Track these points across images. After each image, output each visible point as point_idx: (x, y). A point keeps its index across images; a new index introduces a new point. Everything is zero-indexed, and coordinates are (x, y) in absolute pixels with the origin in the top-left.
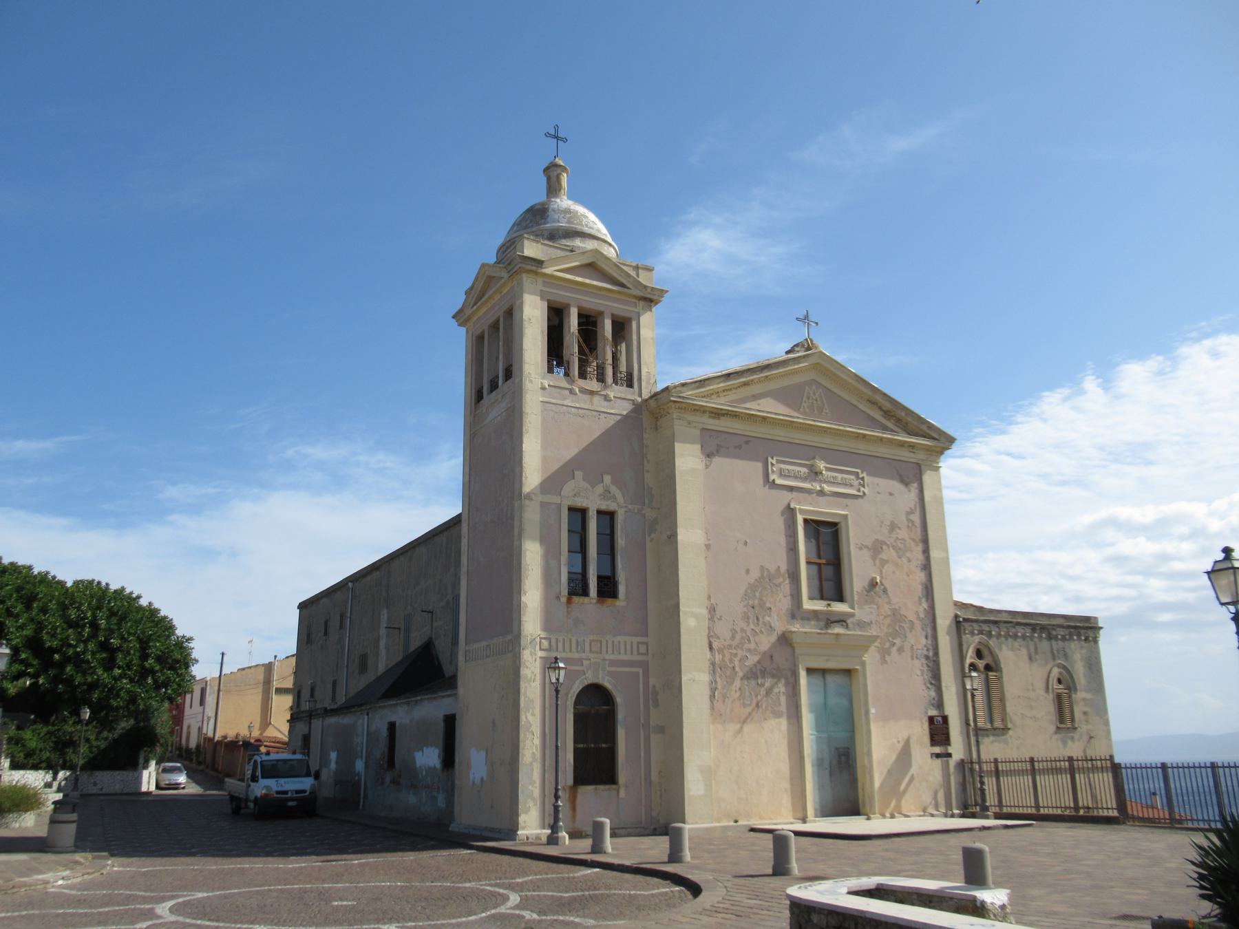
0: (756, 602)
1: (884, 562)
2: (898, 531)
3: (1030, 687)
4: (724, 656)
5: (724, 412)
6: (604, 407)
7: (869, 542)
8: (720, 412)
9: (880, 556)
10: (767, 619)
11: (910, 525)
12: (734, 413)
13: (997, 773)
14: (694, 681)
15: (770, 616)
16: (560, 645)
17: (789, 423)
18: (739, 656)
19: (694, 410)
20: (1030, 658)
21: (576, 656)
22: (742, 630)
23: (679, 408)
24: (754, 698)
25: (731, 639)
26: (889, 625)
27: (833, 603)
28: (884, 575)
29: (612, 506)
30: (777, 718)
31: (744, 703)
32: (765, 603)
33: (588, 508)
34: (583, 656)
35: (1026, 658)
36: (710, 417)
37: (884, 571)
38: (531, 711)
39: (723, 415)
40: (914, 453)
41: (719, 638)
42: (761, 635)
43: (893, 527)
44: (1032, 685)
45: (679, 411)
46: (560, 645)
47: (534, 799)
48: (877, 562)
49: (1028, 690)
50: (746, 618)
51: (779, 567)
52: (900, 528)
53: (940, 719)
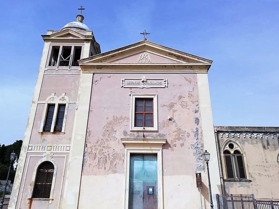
0: (110, 129)
1: (174, 111)
2: (183, 98)
3: (265, 161)
4: (92, 149)
5: (102, 66)
6: (67, 73)
7: (168, 104)
8: (100, 66)
9: (173, 109)
10: (114, 135)
11: (190, 96)
12: (106, 66)
13: (233, 201)
14: (76, 159)
15: (115, 134)
16: (36, 148)
17: (130, 66)
18: (99, 149)
19: (90, 67)
20: (264, 147)
21: (41, 151)
22: (102, 139)
23: (84, 67)
24: (104, 166)
25: (96, 143)
26: (176, 135)
27: (145, 128)
28: (174, 116)
29: (64, 102)
30: (113, 173)
31: (98, 167)
32: (114, 129)
33: (58, 104)
34: (44, 152)
35: (262, 148)
36: (97, 69)
37: (174, 114)
38: (20, 171)
39: (102, 67)
40: (192, 69)
41: (90, 143)
42: (110, 141)
43: (180, 97)
44: (266, 160)
45: (84, 68)
46: (36, 148)
47: (14, 203)
48: (171, 111)
49: (263, 162)
50: (104, 135)
51: (122, 116)
52: (184, 98)
53: (199, 174)
